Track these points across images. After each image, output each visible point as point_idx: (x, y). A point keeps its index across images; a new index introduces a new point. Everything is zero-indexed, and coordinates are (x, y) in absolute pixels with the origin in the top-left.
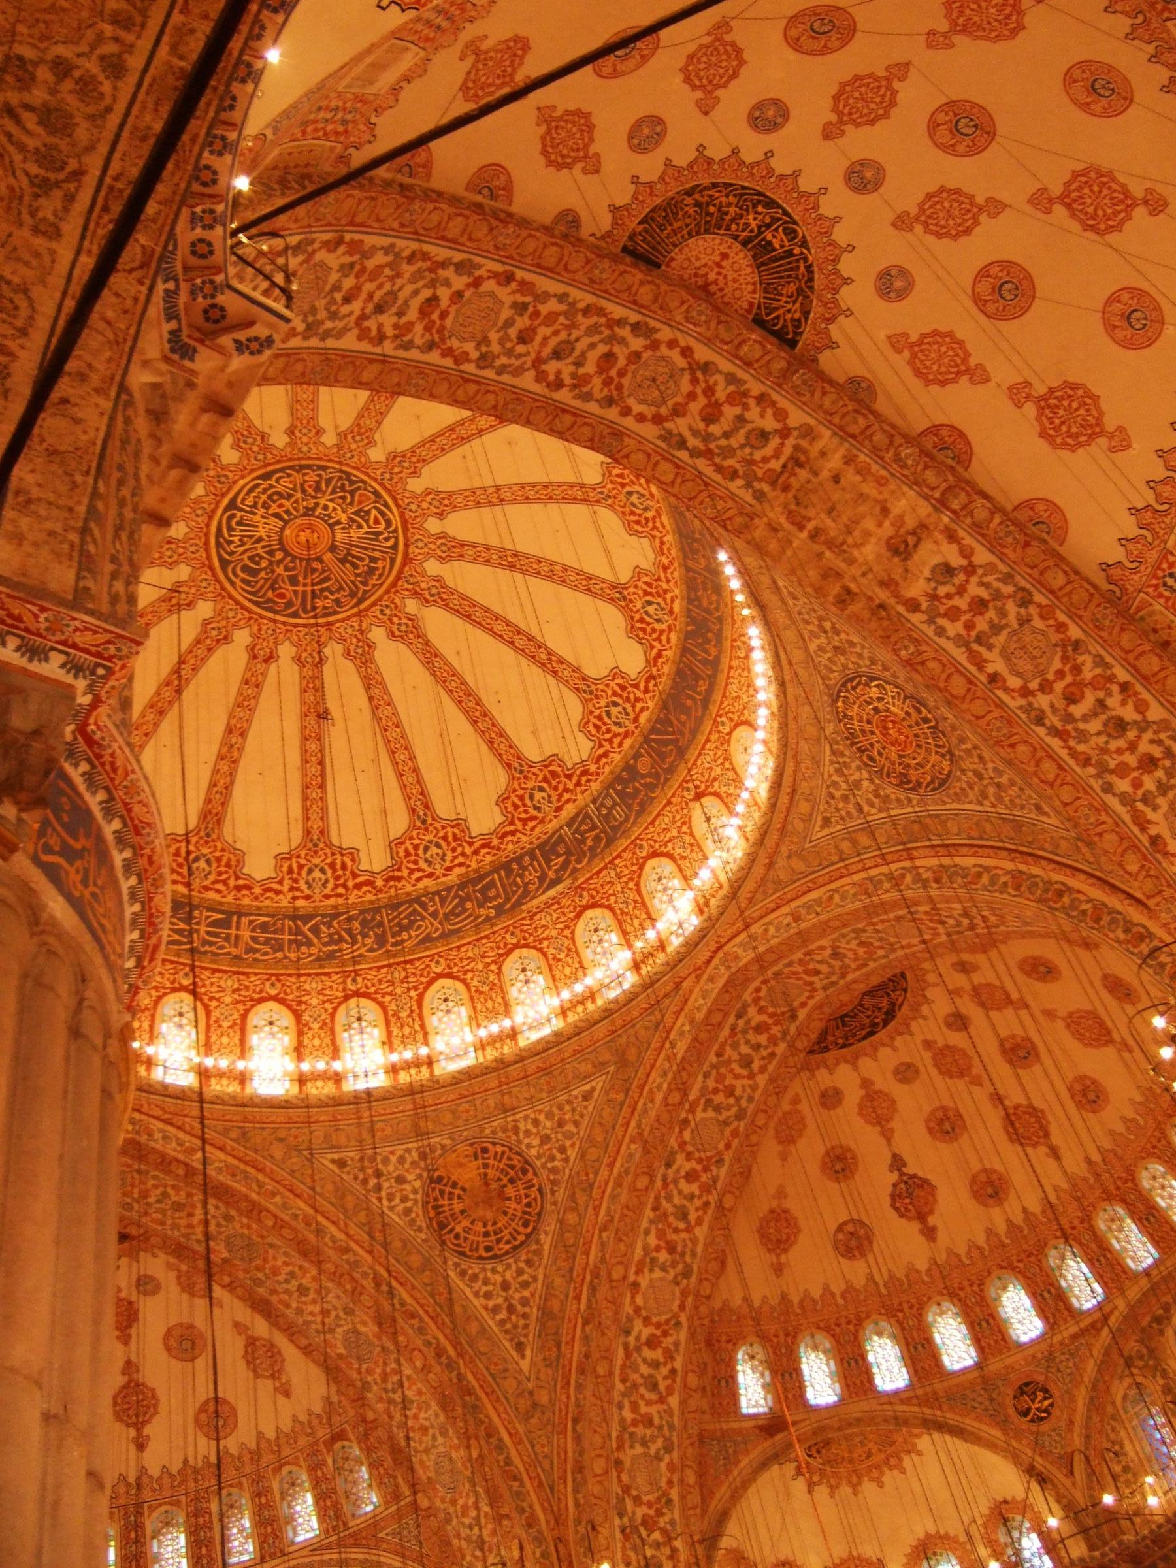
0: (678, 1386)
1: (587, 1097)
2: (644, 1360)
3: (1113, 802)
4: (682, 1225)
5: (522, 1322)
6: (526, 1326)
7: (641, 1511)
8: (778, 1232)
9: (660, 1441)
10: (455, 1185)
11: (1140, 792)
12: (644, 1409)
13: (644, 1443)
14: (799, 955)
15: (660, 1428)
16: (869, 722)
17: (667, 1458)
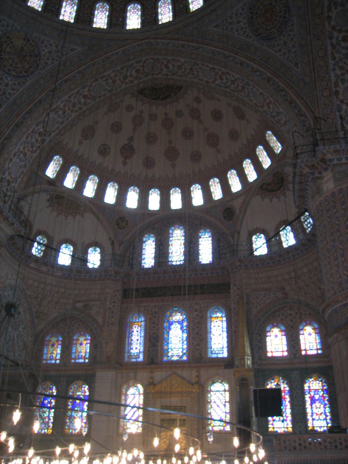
0: (38, 152)
1: (72, 50)
2: (35, 138)
3: (332, 74)
4: (71, 108)
5: (5, 99)
6: (5, 101)
7: (8, 178)
8: (88, 133)
9: (23, 163)
10: (12, 43)
11: (342, 77)
12: (26, 150)
13: (20, 160)
14: (170, 58)
15: (26, 159)
16: (264, 6)
17: (23, 169)
